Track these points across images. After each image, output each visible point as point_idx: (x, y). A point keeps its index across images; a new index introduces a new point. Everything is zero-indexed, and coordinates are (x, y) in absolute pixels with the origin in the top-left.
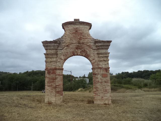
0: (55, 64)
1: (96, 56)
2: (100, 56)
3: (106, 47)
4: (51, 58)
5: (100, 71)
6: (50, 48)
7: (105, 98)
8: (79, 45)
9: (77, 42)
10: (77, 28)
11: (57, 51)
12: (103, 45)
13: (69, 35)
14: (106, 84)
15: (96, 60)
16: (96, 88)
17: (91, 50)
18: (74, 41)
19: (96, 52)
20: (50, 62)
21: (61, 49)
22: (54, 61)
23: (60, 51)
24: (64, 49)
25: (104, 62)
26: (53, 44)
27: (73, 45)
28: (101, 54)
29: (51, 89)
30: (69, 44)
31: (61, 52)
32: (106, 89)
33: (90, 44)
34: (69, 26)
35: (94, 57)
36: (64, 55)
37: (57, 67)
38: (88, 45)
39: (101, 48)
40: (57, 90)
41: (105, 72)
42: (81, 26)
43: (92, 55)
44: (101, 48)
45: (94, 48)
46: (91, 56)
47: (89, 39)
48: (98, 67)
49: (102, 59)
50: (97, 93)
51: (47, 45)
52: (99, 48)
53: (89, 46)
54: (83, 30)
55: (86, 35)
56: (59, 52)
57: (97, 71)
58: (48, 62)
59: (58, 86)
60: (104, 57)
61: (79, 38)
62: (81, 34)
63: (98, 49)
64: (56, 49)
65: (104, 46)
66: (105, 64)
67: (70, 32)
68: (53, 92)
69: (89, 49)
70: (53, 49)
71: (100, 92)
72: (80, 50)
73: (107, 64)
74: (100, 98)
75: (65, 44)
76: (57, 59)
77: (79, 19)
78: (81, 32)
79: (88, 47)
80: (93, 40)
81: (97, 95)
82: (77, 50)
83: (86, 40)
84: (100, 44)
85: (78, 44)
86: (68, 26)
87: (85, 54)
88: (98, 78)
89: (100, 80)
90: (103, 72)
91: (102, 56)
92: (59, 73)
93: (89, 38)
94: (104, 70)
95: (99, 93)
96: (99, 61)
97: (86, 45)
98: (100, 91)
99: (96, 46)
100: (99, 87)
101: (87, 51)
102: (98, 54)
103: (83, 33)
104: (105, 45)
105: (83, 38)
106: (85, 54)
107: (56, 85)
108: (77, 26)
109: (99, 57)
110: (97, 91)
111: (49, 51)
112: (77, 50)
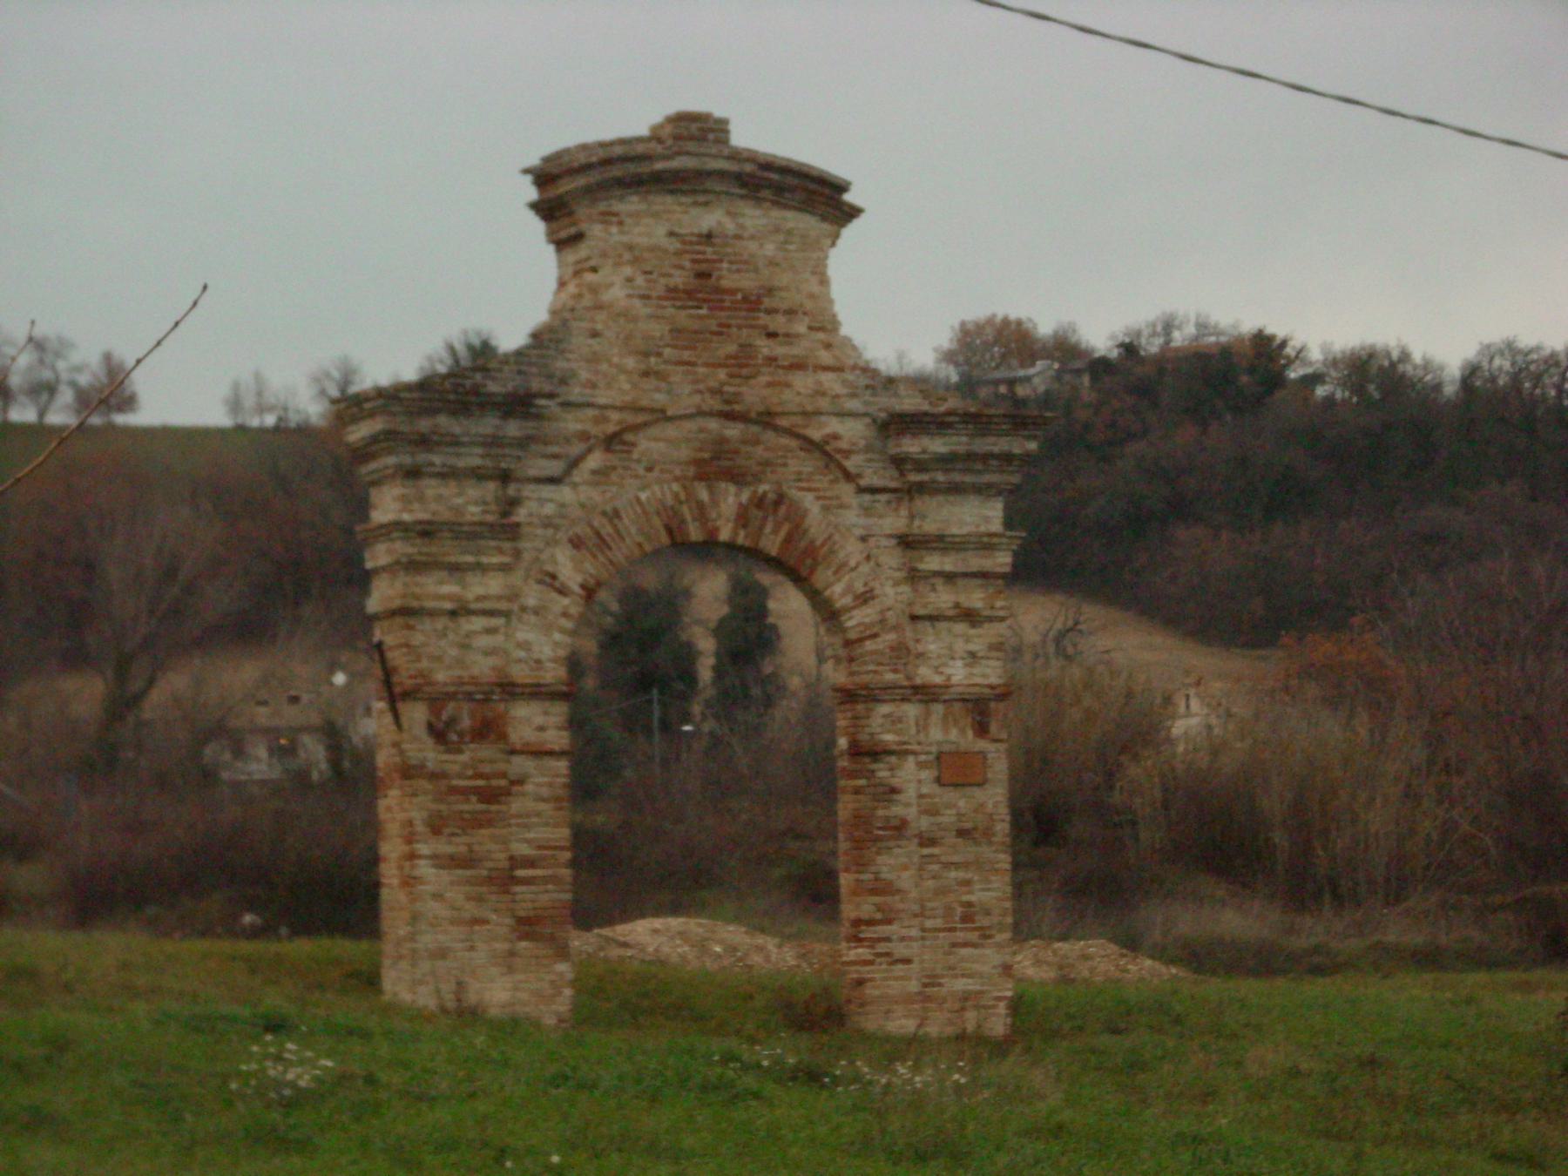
0: (497, 640)
1: (891, 559)
2: (933, 562)
3: (987, 478)
4: (455, 569)
5: (922, 726)
6: (453, 461)
7: (961, 985)
8: (733, 431)
9: (715, 404)
10: (708, 237)
11: (512, 490)
12: (970, 457)
13: (626, 315)
14: (967, 851)
15: (889, 602)
16: (882, 888)
17: (846, 490)
18: (683, 394)
19: (894, 522)
20: (453, 614)
21: (554, 468)
22: (487, 605)
23: (547, 491)
24: (578, 476)
25: (961, 628)
26: (487, 425)
27: (671, 431)
28: (940, 542)
29: (469, 898)
30: (631, 418)
31: (549, 509)
32: (970, 904)
33: (834, 425)
34: (631, 204)
35: (865, 568)
36: (577, 543)
37: (521, 674)
38: (816, 434)
39: (940, 477)
40: (528, 898)
41: (962, 731)
42: (754, 217)
43: (851, 550)
44: (940, 477)
45: (876, 481)
46: (841, 555)
47: (826, 369)
48: (899, 678)
49: (943, 598)
50: (880, 940)
51: (424, 425)
52: (924, 477)
53: (826, 453)
54: (772, 263)
55: (801, 328)
56: (537, 504)
57: (895, 721)
58: (432, 614)
59: (530, 863)
60: (965, 575)
61: (728, 357)
62: (752, 303)
63: (921, 489)
64: (505, 477)
65: (979, 466)
66: (973, 655)
67: (640, 280)
68: (484, 922)
69: (822, 482)
70: (478, 475)
71: (914, 932)
72: (732, 489)
74: (914, 986)
75: (590, 412)
76: (516, 578)
77: (718, 112)
78: (746, 282)
79: (804, 464)
80: (863, 381)
81: (888, 954)
82: (704, 495)
83: (802, 382)
84: (938, 445)
85: (713, 424)
86: (618, 207)
87: (783, 533)
88: (894, 791)
89: (911, 813)
90: (946, 731)
91: (948, 563)
92: (541, 729)
93: (825, 357)
94: (957, 706)
95: (903, 939)
96: (914, 618)
97: (798, 436)
98: (916, 921)
99: (899, 462)
100: (906, 880)
101: (809, 501)
102: (907, 542)
103: (767, 302)
104: (986, 457)
105: (771, 360)
106: (788, 540)
107: (512, 858)
108: (710, 219)
109: (914, 576)
110: (889, 922)
111: (431, 488)
112: (704, 495)
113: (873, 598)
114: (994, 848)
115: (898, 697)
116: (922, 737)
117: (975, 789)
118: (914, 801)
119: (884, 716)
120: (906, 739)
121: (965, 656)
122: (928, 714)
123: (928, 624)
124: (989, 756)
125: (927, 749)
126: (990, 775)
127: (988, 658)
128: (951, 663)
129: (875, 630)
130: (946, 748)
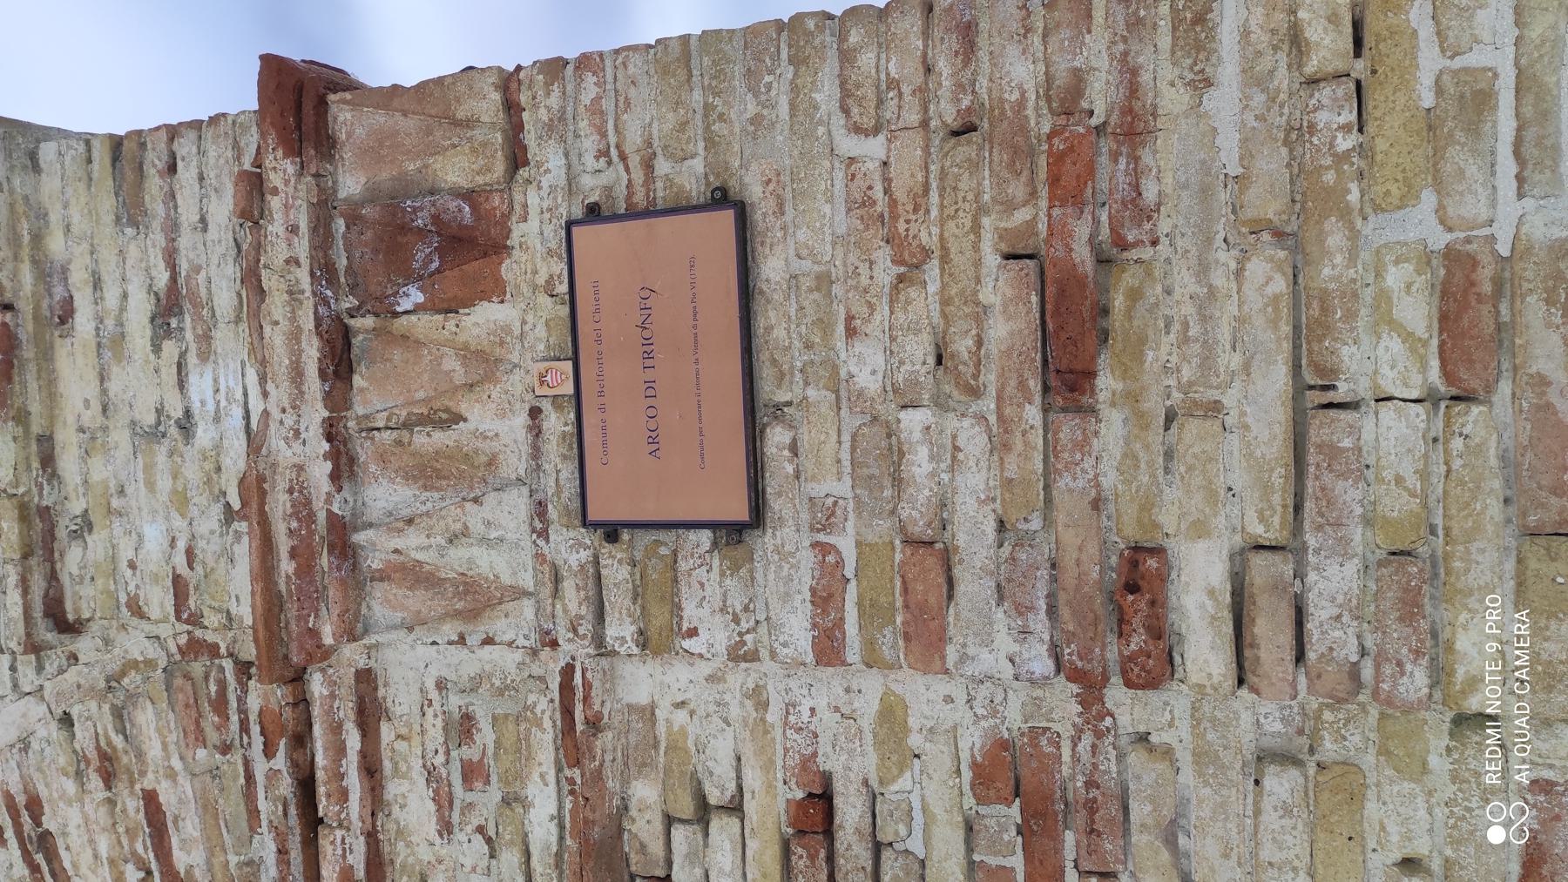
73: (132, 213)
113: (35, 806)
114: (1172, 99)
115: (353, 741)
116: (518, 622)
117: (772, 268)
118: (871, 687)
119: (446, 828)
120: (545, 705)
121: (170, 348)
122: (415, 575)
123: (72, 559)
124: (592, 186)
125: (573, 599)
126: (691, 177)
127: (172, 228)
128: (204, 434)
129: (133, 806)
130: (559, 471)
